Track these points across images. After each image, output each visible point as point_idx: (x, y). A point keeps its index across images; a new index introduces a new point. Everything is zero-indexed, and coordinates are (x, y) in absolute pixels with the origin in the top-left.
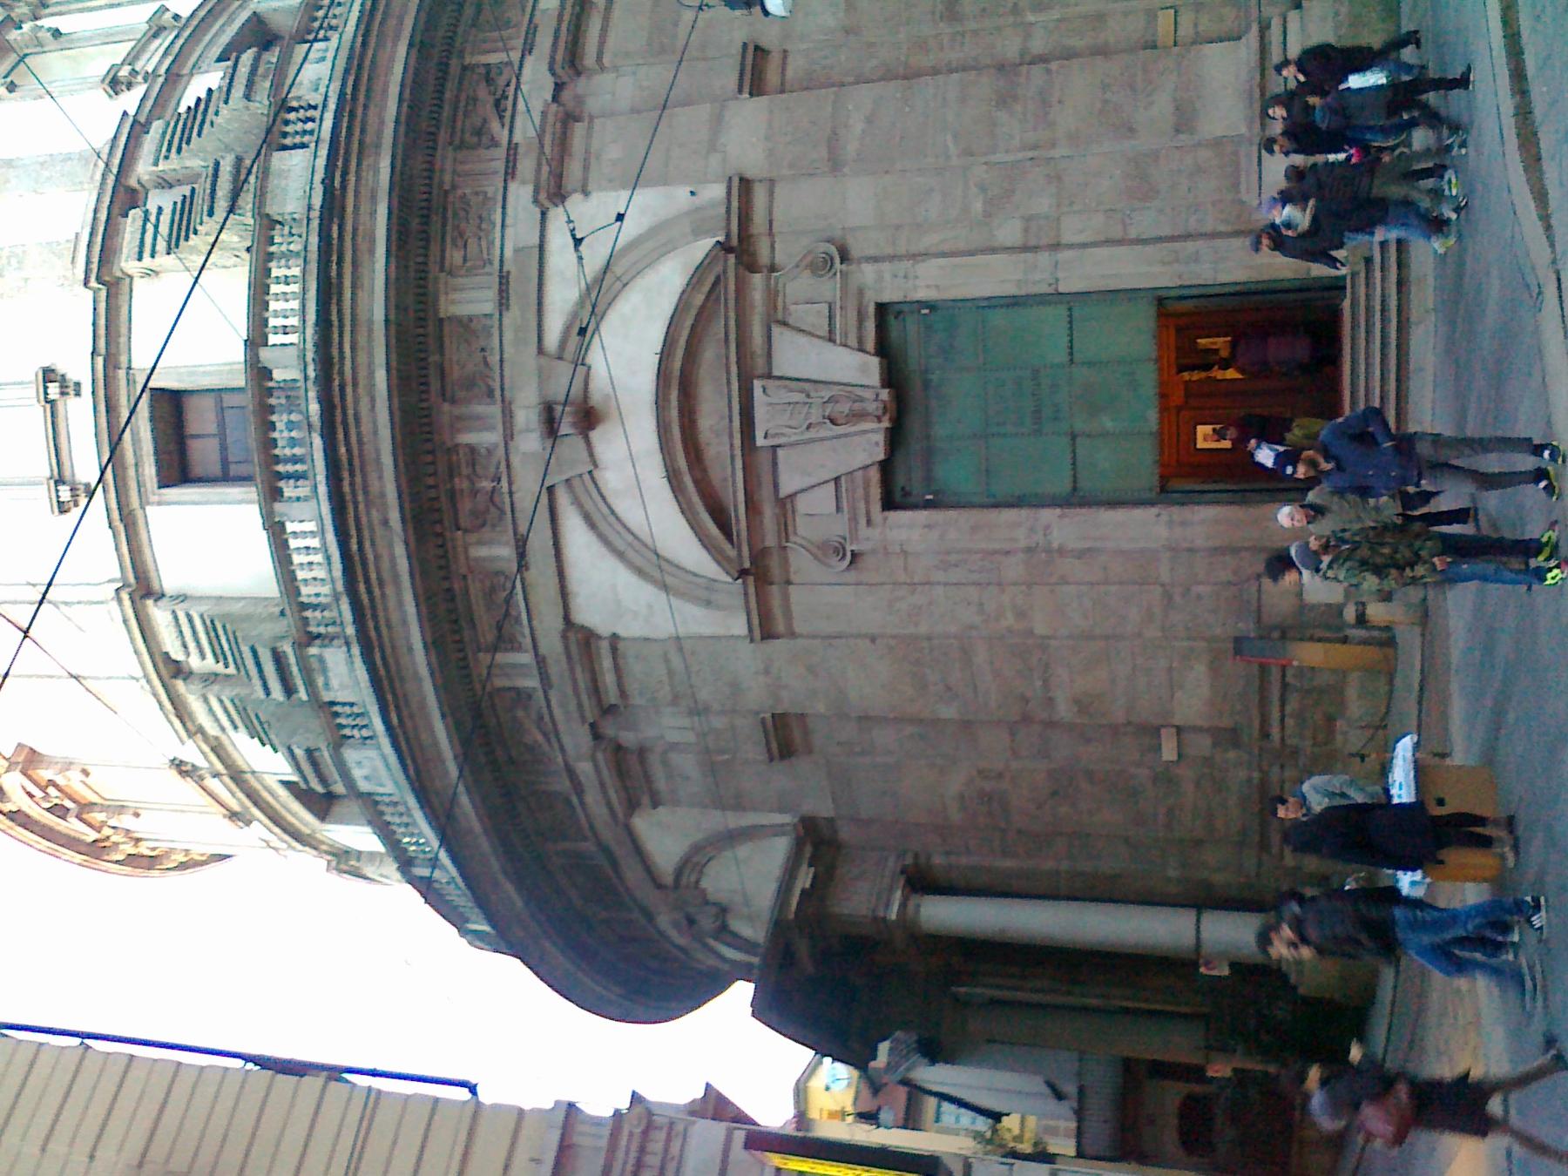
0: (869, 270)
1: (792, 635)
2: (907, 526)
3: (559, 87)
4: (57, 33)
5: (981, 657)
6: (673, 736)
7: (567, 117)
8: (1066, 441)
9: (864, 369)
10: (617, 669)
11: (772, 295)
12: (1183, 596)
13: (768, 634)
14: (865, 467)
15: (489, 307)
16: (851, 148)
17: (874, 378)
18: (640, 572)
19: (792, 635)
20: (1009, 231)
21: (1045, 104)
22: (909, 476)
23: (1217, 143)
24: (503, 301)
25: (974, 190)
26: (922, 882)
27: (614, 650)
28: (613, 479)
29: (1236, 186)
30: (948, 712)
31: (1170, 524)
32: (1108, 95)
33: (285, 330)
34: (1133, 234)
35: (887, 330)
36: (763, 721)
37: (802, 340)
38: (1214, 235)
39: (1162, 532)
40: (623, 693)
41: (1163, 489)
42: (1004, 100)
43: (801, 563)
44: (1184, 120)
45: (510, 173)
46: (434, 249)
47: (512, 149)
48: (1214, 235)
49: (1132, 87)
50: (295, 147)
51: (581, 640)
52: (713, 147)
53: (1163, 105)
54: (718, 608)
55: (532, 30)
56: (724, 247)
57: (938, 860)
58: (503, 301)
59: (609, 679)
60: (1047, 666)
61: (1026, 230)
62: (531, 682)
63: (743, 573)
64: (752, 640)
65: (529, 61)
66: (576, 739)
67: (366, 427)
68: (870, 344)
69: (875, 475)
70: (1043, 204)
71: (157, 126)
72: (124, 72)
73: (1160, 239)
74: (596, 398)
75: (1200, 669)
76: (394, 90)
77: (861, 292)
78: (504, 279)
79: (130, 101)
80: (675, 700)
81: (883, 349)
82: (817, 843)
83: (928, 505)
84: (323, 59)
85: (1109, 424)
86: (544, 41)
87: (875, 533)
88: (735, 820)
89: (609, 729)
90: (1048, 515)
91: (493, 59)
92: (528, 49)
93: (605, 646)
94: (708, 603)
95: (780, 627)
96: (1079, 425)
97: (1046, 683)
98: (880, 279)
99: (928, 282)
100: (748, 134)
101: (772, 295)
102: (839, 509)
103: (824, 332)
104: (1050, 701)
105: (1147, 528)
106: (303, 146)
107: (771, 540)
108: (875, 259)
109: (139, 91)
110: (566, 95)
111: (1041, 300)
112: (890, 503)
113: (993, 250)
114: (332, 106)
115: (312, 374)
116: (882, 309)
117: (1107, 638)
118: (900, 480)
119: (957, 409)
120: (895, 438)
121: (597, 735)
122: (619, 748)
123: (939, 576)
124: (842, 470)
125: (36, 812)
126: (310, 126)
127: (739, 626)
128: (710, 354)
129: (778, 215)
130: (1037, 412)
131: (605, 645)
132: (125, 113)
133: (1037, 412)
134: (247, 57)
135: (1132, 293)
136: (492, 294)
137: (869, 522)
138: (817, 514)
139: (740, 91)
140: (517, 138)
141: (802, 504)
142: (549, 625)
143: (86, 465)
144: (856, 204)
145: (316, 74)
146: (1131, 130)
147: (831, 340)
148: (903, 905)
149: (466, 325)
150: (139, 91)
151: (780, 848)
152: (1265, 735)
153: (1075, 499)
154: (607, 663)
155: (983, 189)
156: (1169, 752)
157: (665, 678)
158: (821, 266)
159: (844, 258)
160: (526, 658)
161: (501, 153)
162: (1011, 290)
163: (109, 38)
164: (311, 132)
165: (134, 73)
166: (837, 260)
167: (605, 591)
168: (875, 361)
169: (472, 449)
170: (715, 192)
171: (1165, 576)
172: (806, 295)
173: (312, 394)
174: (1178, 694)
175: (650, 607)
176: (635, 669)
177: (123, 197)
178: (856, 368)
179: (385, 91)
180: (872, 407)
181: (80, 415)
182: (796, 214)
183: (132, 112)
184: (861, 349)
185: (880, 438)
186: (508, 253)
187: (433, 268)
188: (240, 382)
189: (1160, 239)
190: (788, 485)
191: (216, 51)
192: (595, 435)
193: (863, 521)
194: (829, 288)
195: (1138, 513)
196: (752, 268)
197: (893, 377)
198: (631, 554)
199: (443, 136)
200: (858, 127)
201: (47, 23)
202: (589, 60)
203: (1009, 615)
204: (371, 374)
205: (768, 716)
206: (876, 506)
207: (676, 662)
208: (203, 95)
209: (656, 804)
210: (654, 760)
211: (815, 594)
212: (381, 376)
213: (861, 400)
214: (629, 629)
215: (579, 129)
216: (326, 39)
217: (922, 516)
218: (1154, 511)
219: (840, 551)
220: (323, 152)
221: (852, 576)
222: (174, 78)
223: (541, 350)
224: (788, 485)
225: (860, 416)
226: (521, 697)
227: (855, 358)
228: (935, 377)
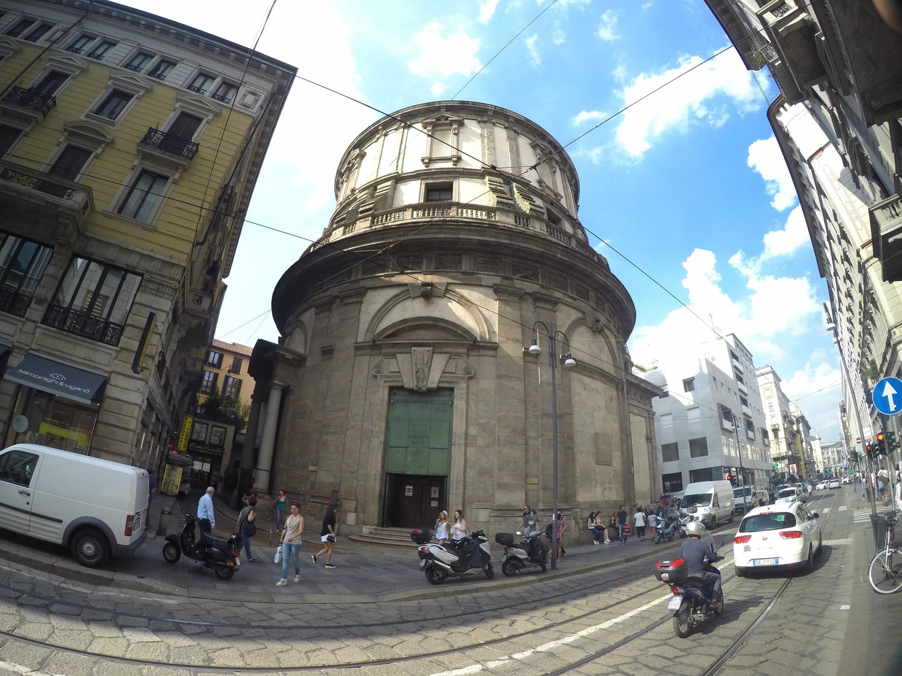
0: (465, 386)
1: (355, 356)
2: (383, 393)
3: (530, 294)
4: (555, 172)
6: (333, 319)
7: (522, 296)
9: (433, 382)
10: (352, 303)
11: (459, 355)
13: (356, 349)
15: (463, 269)
16: (504, 382)
17: (430, 385)
18: (379, 310)
19: (355, 356)
20: (473, 431)
21: (512, 443)
22: (400, 396)
23: (493, 495)
24: (464, 273)
26: (285, 392)
27: (358, 302)
28: (408, 303)
30: (328, 402)
33: (462, 213)
34: (468, 469)
35: (445, 391)
37: (444, 364)
38: (464, 494)
39: (373, 473)
40: (345, 305)
42: (515, 431)
43: (378, 359)
44: (502, 486)
45: (504, 278)
47: (512, 279)
48: (464, 494)
51: (362, 293)
52: (508, 339)
53: (507, 480)
55: (548, 289)
56: (475, 340)
57: (292, 397)
58: (464, 273)
59: (350, 301)
62: (353, 278)
63: (374, 341)
65: (538, 287)
66: (335, 291)
68: (441, 385)
69: (400, 384)
70: (480, 442)
73: (465, 477)
75: (332, 480)
76: (529, 246)
77: (458, 383)
78: (472, 274)
80: (342, 320)
81: (439, 389)
83: (389, 400)
86: (544, 291)
87: (382, 383)
88: (309, 336)
89: (338, 301)
90: (382, 438)
91: (540, 277)
92: (542, 286)
93: (360, 299)
94: (367, 331)
95: (358, 353)
96: (409, 449)
97: (332, 433)
98: (462, 389)
99: (459, 404)
104: (327, 434)
105: (374, 467)
107: (383, 351)
108: (468, 388)
109: (538, 187)
110: (528, 296)
111: (450, 440)
112: (391, 389)
113: (467, 425)
116: (452, 389)
117: (343, 452)
118: (399, 392)
119: (417, 411)
120: (411, 391)
121: (337, 297)
122: (332, 303)
123: (367, 403)
125: (350, 158)
127: (360, 340)
128: (443, 335)
129: (485, 358)
131: (360, 299)
135: (449, 467)
136: (467, 270)
138: (391, 365)
140: (515, 281)
141: (393, 361)
142: (368, 283)
144: (486, 383)
148: (278, 385)
149: (459, 263)
150: (538, 187)
151: (301, 350)
152: (313, 497)
153: (386, 446)
154: (355, 300)
156: (311, 468)
158: (467, 371)
159: (470, 378)
160: (359, 277)
161: (511, 276)
162: (454, 431)
163: (555, 183)
167: (376, 300)
168: (435, 386)
169: (421, 263)
171: (360, 472)
177: (508, 179)
178: (434, 379)
181: (449, 165)
182: (486, 365)
185: (411, 386)
189: (465, 477)
190: (398, 356)
192: (422, 299)
194: (460, 373)
195: (379, 465)
196: (468, 349)
197: (430, 392)
199: (516, 260)
200: (510, 385)
201: (558, 170)
202: (538, 304)
207: (353, 320)
209: (316, 314)
210: (327, 314)
211: (366, 363)
212: (443, 236)
213: (423, 380)
214: (364, 307)
215: (517, 299)
217: (386, 398)
219: (378, 372)
221: (370, 376)
222: (541, 196)
223: (448, 284)
224: (398, 356)
225: (418, 381)
226: (349, 275)
228: (430, 405)
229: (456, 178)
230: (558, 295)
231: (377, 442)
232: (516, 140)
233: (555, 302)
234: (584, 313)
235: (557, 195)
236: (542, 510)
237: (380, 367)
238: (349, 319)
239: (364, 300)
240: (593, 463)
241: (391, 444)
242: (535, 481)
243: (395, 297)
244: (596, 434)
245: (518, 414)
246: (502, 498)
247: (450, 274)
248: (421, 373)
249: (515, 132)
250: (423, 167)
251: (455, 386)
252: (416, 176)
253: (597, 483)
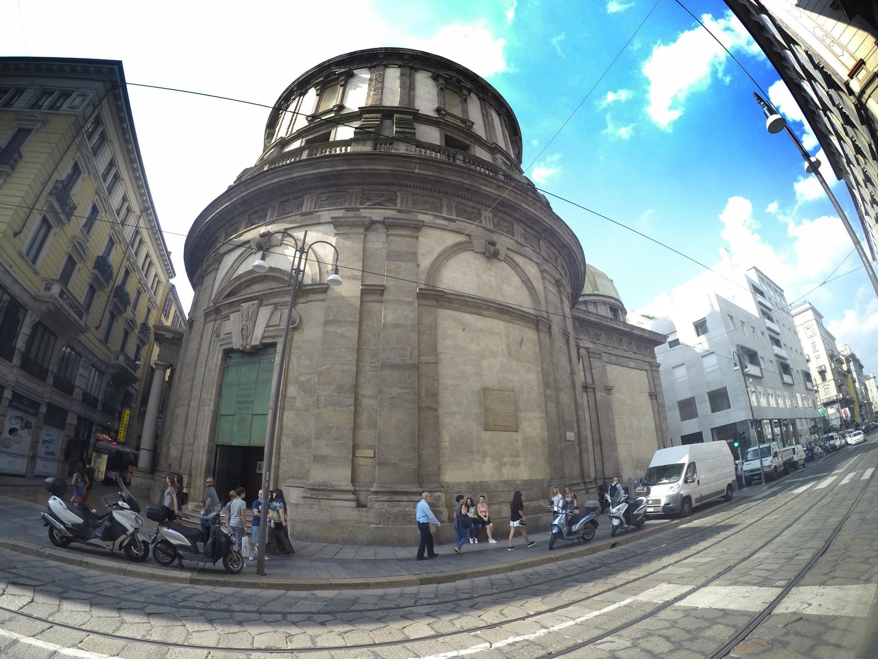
9: (256, 339)
11: (284, 304)
16: (331, 329)
17: (253, 343)
21: (336, 404)
22: (235, 358)
23: (308, 472)
25: (309, 377)
29: (293, 478)
32: (334, 429)
41: (217, 446)
42: (340, 388)
44: (319, 459)
45: (347, 210)
46: (324, 190)
47: (358, 209)
49: (337, 439)
53: (326, 450)
61: (292, 398)
67: (264, 179)
68: (265, 341)
70: (299, 404)
74: (272, 250)
76: (373, 167)
78: (311, 213)
85: (235, 428)
91: (399, 201)
101: (284, 304)
103: (271, 324)
105: (203, 440)
118: (234, 356)
129: (314, 303)
130: (241, 402)
133: (241, 402)
140: (362, 211)
144: (311, 334)
146: (318, 438)
147: (267, 326)
155: (309, 380)
178: (257, 337)
179: (372, 164)
184: (263, 338)
186: (319, 213)
187: (319, 191)
191: (450, 134)
199: (365, 187)
200: (339, 331)
202: (390, 232)
204: (278, 177)
212: (277, 180)
229: (333, 127)
230: (421, 217)
233: (418, 227)
234: (469, 236)
236: (375, 493)
241: (223, 412)
242: (370, 453)
243: (240, 256)
244: (485, 390)
245: (346, 367)
246: (319, 475)
247: (288, 219)
253: (485, 455)
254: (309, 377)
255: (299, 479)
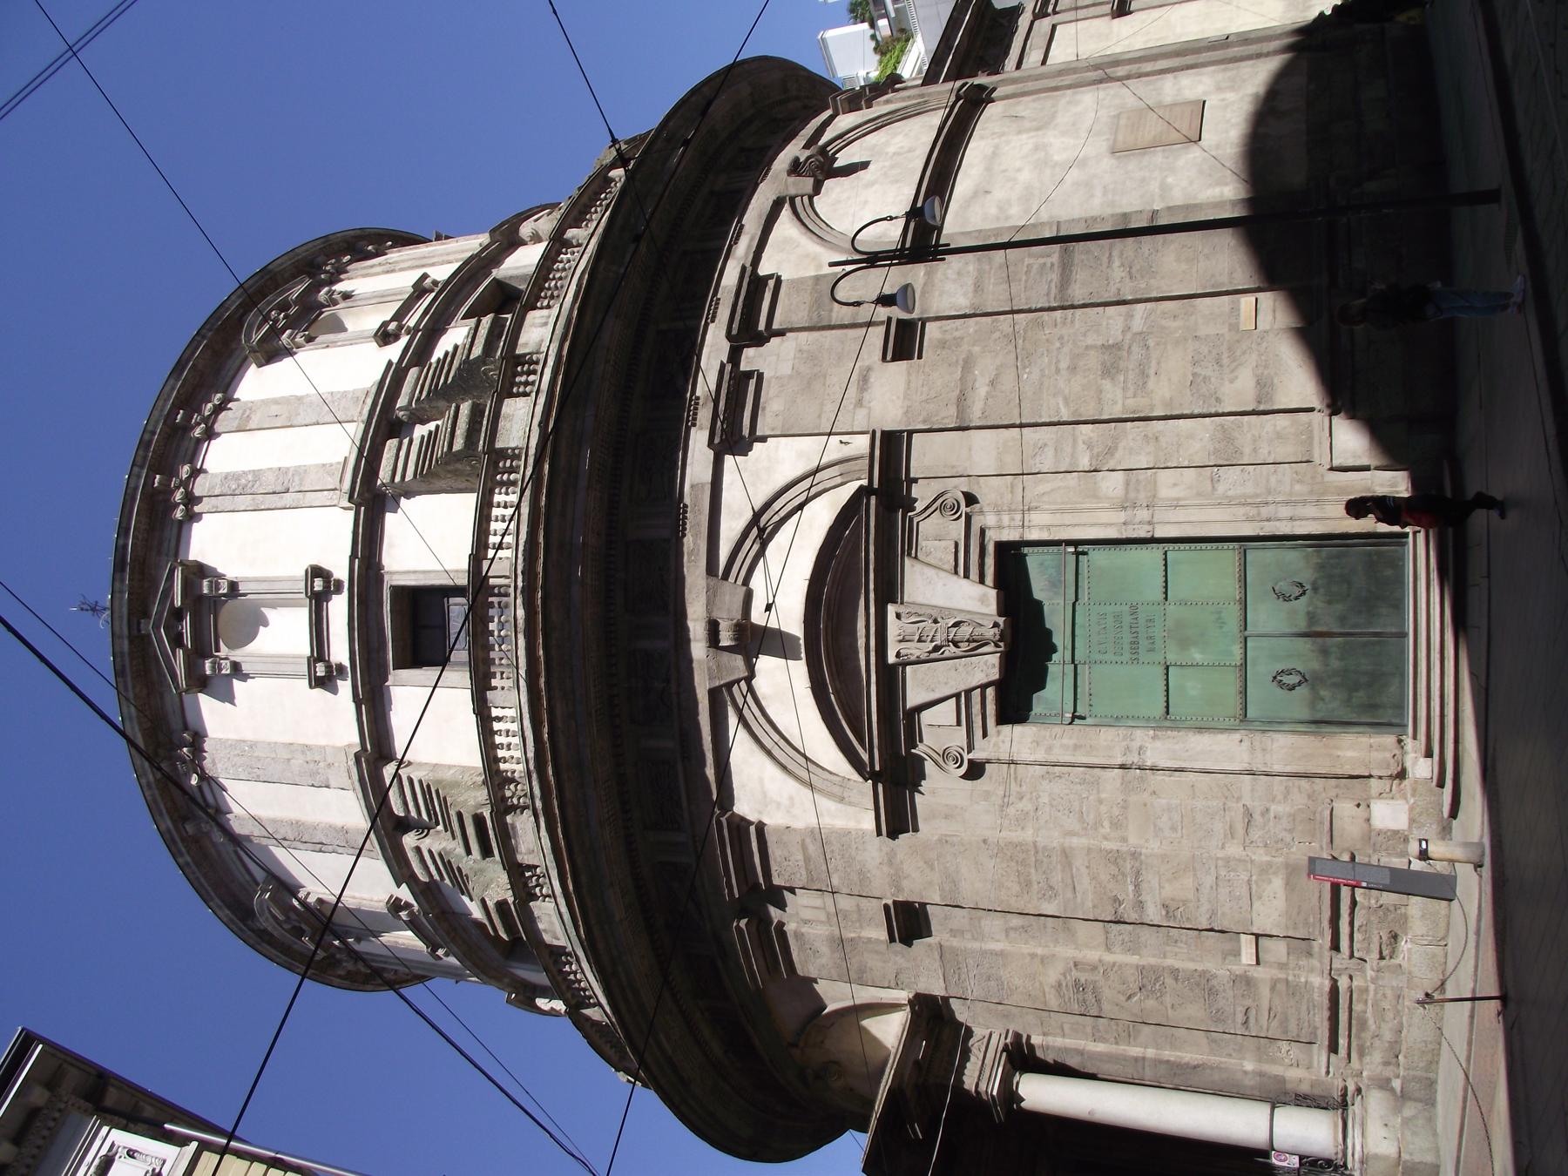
5: (1079, 863)
8: (1161, 670)
9: (983, 600)
12: (1263, 815)
14: (983, 687)
17: (991, 607)
21: (1144, 374)
25: (1081, 446)
31: (1252, 749)
36: (886, 907)
50: (518, 395)
54: (850, 804)
60: (1138, 873)
64: (879, 833)
71: (413, 372)
72: (393, 326)
75: (1278, 883)
77: (983, 532)
79: (394, 351)
82: (933, 1020)
84: (546, 324)
85: (1197, 656)
90: (1141, 736)
93: (752, 829)
94: (842, 800)
96: (1172, 658)
100: (891, 395)
102: (959, 723)
104: (1140, 905)
106: (526, 394)
114: (551, 363)
115: (520, 584)
124: (963, 687)
126: (531, 378)
127: (868, 822)
130: (1135, 644)
131: (752, 829)
132: (390, 363)
133: (1135, 644)
134: (487, 321)
137: (985, 735)
139: (884, 359)
141: (926, 717)
143: (340, 651)
145: (539, 332)
150: (404, 340)
152: (1335, 946)
153: (1168, 718)
155: (1090, 447)
157: (801, 863)
163: (381, 298)
164: (533, 383)
165: (400, 327)
166: (963, 504)
168: (993, 593)
170: (861, 444)
172: (936, 535)
173: (519, 601)
174: (1256, 905)
175: (791, 798)
176: (775, 852)
178: (976, 601)
180: (990, 633)
183: (395, 360)
184: (982, 581)
188: (463, 580)
191: (464, 310)
193: (978, 732)
195: (1222, 738)
198: (776, 752)
200: (982, 390)
201: (339, 287)
203: (1106, 824)
205: (890, 902)
206: (991, 721)
208: (450, 349)
216: (548, 307)
218: (1237, 736)
220: (542, 400)
227: (979, 589)
229: (380, 579)
231: (1158, 749)
232: (252, 407)
235: (419, 290)
237: (945, 754)
238: (807, 859)
239: (753, 817)
240: (1194, 153)
248: (954, 643)
249: (219, 409)
250: (345, 687)
251: (993, 537)
252: (373, 706)
254: (1081, 446)
255: (1311, 438)
